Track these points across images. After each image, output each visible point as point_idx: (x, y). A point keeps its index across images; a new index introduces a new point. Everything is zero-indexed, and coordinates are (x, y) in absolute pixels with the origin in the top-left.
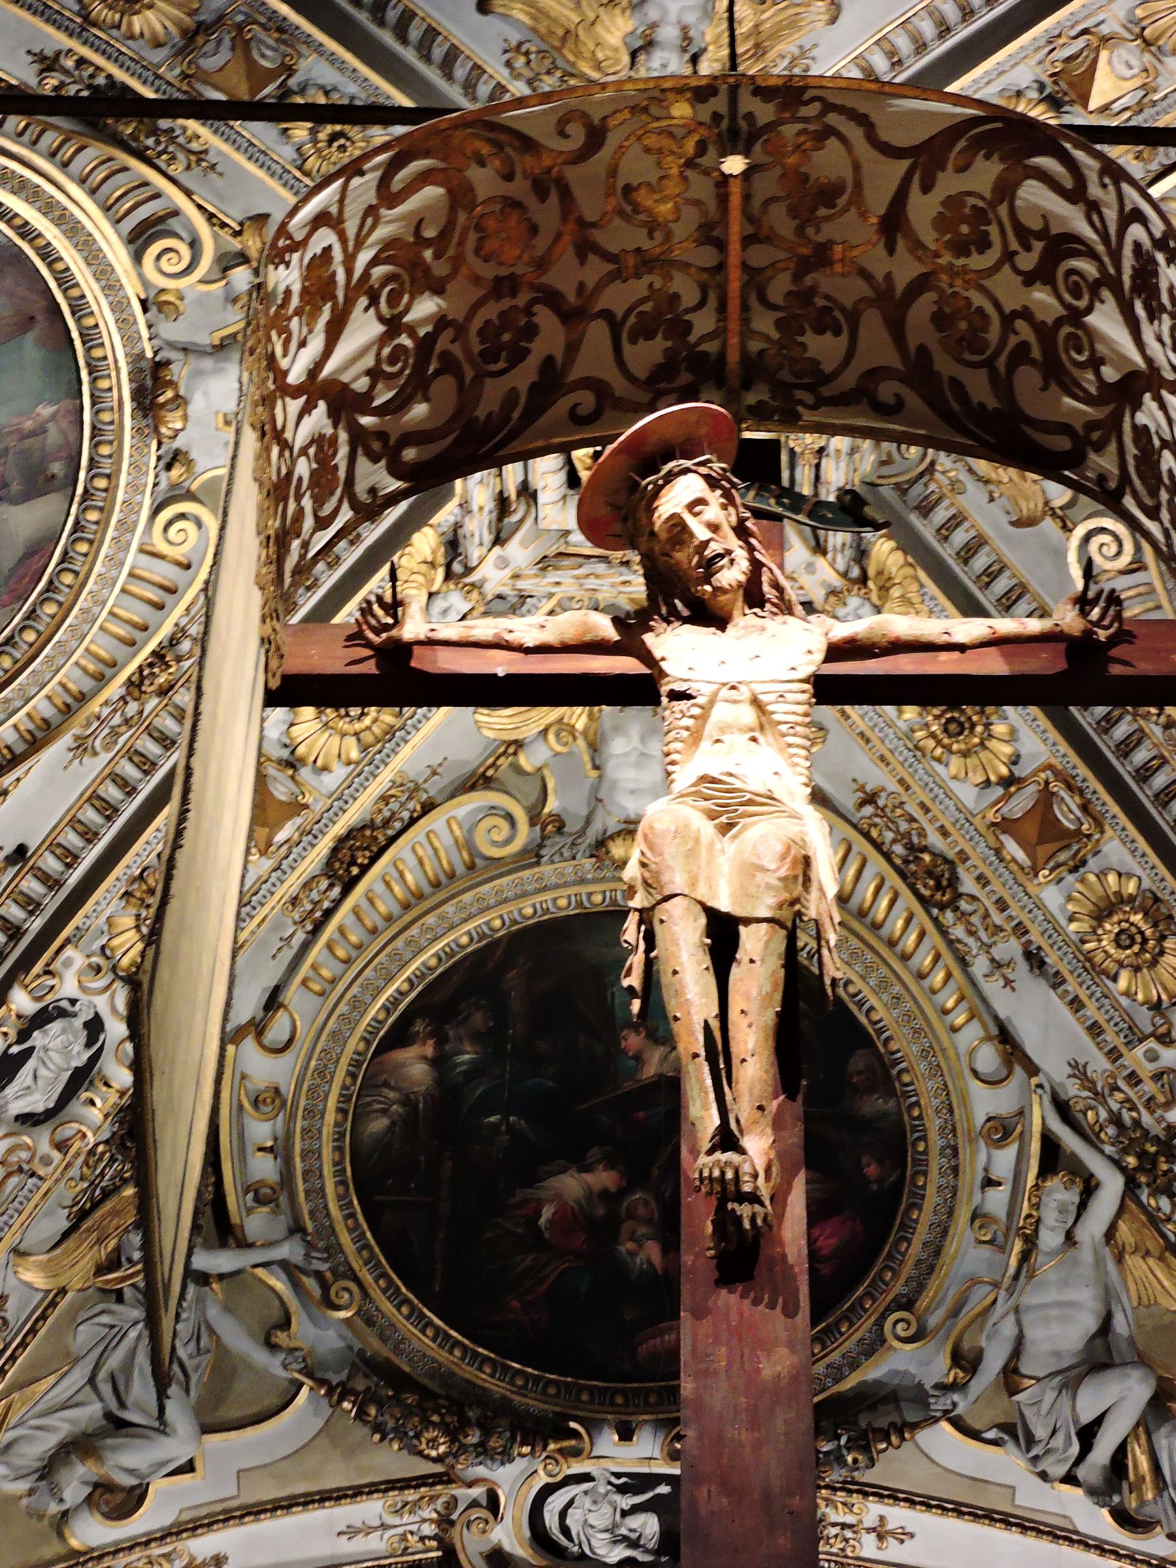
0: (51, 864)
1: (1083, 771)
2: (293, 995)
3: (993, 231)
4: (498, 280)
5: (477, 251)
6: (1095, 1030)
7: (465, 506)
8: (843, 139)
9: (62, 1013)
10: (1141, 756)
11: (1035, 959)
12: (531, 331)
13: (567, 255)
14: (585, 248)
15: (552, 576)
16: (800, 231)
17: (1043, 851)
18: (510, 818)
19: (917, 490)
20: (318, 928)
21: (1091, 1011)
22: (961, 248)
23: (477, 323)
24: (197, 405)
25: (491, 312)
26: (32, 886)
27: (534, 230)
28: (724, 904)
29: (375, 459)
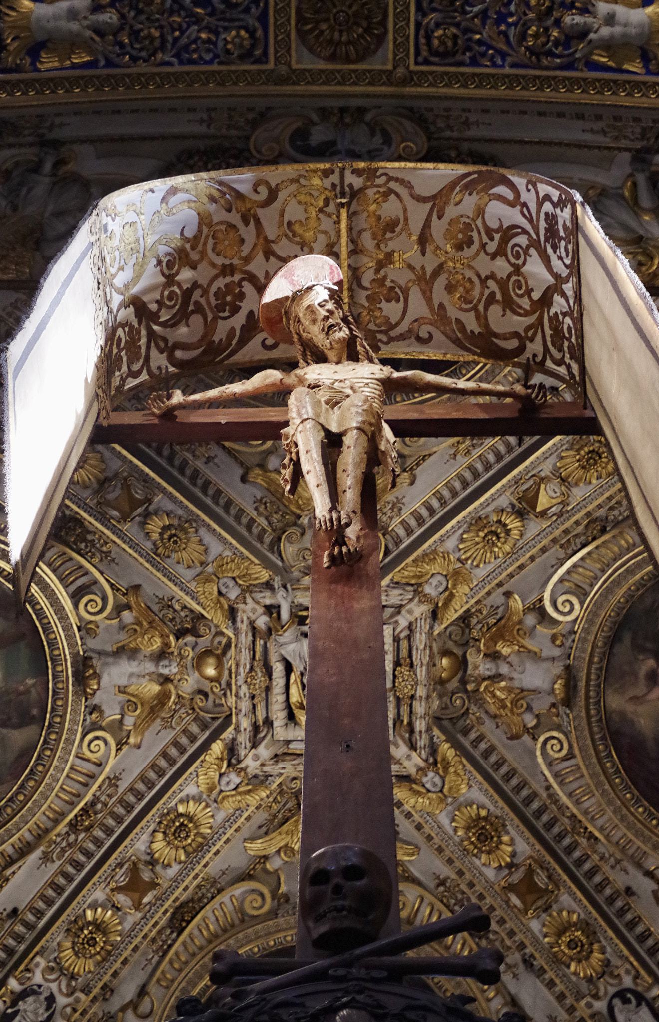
0: (30, 917)
1: (548, 858)
2: (153, 988)
3: (475, 234)
4: (224, 266)
5: (213, 250)
6: (561, 997)
7: (237, 729)
8: (398, 195)
9: (34, 993)
10: (577, 854)
11: (528, 962)
12: (241, 296)
13: (260, 256)
14: (268, 253)
15: (281, 765)
16: (378, 246)
17: (530, 898)
18: (262, 895)
19: (461, 723)
20: (165, 953)
21: (560, 987)
22: (459, 247)
23: (213, 289)
24: (105, 679)
25: (220, 283)
26: (20, 928)
27: (242, 241)
28: (334, 428)
29: (161, 352)
